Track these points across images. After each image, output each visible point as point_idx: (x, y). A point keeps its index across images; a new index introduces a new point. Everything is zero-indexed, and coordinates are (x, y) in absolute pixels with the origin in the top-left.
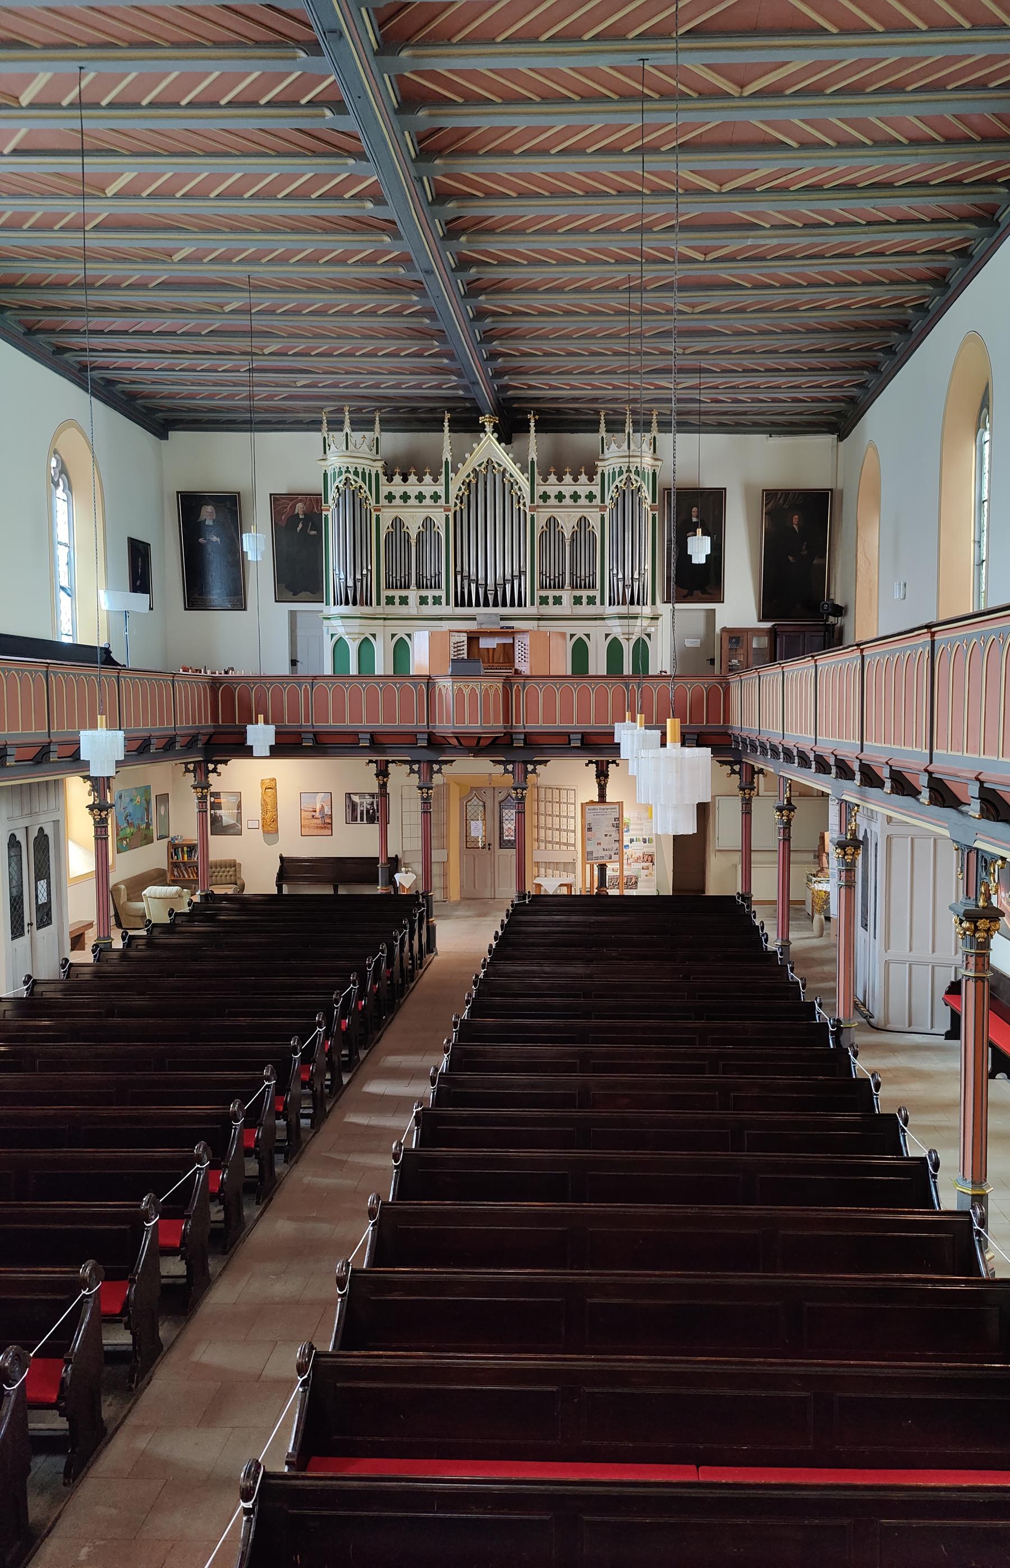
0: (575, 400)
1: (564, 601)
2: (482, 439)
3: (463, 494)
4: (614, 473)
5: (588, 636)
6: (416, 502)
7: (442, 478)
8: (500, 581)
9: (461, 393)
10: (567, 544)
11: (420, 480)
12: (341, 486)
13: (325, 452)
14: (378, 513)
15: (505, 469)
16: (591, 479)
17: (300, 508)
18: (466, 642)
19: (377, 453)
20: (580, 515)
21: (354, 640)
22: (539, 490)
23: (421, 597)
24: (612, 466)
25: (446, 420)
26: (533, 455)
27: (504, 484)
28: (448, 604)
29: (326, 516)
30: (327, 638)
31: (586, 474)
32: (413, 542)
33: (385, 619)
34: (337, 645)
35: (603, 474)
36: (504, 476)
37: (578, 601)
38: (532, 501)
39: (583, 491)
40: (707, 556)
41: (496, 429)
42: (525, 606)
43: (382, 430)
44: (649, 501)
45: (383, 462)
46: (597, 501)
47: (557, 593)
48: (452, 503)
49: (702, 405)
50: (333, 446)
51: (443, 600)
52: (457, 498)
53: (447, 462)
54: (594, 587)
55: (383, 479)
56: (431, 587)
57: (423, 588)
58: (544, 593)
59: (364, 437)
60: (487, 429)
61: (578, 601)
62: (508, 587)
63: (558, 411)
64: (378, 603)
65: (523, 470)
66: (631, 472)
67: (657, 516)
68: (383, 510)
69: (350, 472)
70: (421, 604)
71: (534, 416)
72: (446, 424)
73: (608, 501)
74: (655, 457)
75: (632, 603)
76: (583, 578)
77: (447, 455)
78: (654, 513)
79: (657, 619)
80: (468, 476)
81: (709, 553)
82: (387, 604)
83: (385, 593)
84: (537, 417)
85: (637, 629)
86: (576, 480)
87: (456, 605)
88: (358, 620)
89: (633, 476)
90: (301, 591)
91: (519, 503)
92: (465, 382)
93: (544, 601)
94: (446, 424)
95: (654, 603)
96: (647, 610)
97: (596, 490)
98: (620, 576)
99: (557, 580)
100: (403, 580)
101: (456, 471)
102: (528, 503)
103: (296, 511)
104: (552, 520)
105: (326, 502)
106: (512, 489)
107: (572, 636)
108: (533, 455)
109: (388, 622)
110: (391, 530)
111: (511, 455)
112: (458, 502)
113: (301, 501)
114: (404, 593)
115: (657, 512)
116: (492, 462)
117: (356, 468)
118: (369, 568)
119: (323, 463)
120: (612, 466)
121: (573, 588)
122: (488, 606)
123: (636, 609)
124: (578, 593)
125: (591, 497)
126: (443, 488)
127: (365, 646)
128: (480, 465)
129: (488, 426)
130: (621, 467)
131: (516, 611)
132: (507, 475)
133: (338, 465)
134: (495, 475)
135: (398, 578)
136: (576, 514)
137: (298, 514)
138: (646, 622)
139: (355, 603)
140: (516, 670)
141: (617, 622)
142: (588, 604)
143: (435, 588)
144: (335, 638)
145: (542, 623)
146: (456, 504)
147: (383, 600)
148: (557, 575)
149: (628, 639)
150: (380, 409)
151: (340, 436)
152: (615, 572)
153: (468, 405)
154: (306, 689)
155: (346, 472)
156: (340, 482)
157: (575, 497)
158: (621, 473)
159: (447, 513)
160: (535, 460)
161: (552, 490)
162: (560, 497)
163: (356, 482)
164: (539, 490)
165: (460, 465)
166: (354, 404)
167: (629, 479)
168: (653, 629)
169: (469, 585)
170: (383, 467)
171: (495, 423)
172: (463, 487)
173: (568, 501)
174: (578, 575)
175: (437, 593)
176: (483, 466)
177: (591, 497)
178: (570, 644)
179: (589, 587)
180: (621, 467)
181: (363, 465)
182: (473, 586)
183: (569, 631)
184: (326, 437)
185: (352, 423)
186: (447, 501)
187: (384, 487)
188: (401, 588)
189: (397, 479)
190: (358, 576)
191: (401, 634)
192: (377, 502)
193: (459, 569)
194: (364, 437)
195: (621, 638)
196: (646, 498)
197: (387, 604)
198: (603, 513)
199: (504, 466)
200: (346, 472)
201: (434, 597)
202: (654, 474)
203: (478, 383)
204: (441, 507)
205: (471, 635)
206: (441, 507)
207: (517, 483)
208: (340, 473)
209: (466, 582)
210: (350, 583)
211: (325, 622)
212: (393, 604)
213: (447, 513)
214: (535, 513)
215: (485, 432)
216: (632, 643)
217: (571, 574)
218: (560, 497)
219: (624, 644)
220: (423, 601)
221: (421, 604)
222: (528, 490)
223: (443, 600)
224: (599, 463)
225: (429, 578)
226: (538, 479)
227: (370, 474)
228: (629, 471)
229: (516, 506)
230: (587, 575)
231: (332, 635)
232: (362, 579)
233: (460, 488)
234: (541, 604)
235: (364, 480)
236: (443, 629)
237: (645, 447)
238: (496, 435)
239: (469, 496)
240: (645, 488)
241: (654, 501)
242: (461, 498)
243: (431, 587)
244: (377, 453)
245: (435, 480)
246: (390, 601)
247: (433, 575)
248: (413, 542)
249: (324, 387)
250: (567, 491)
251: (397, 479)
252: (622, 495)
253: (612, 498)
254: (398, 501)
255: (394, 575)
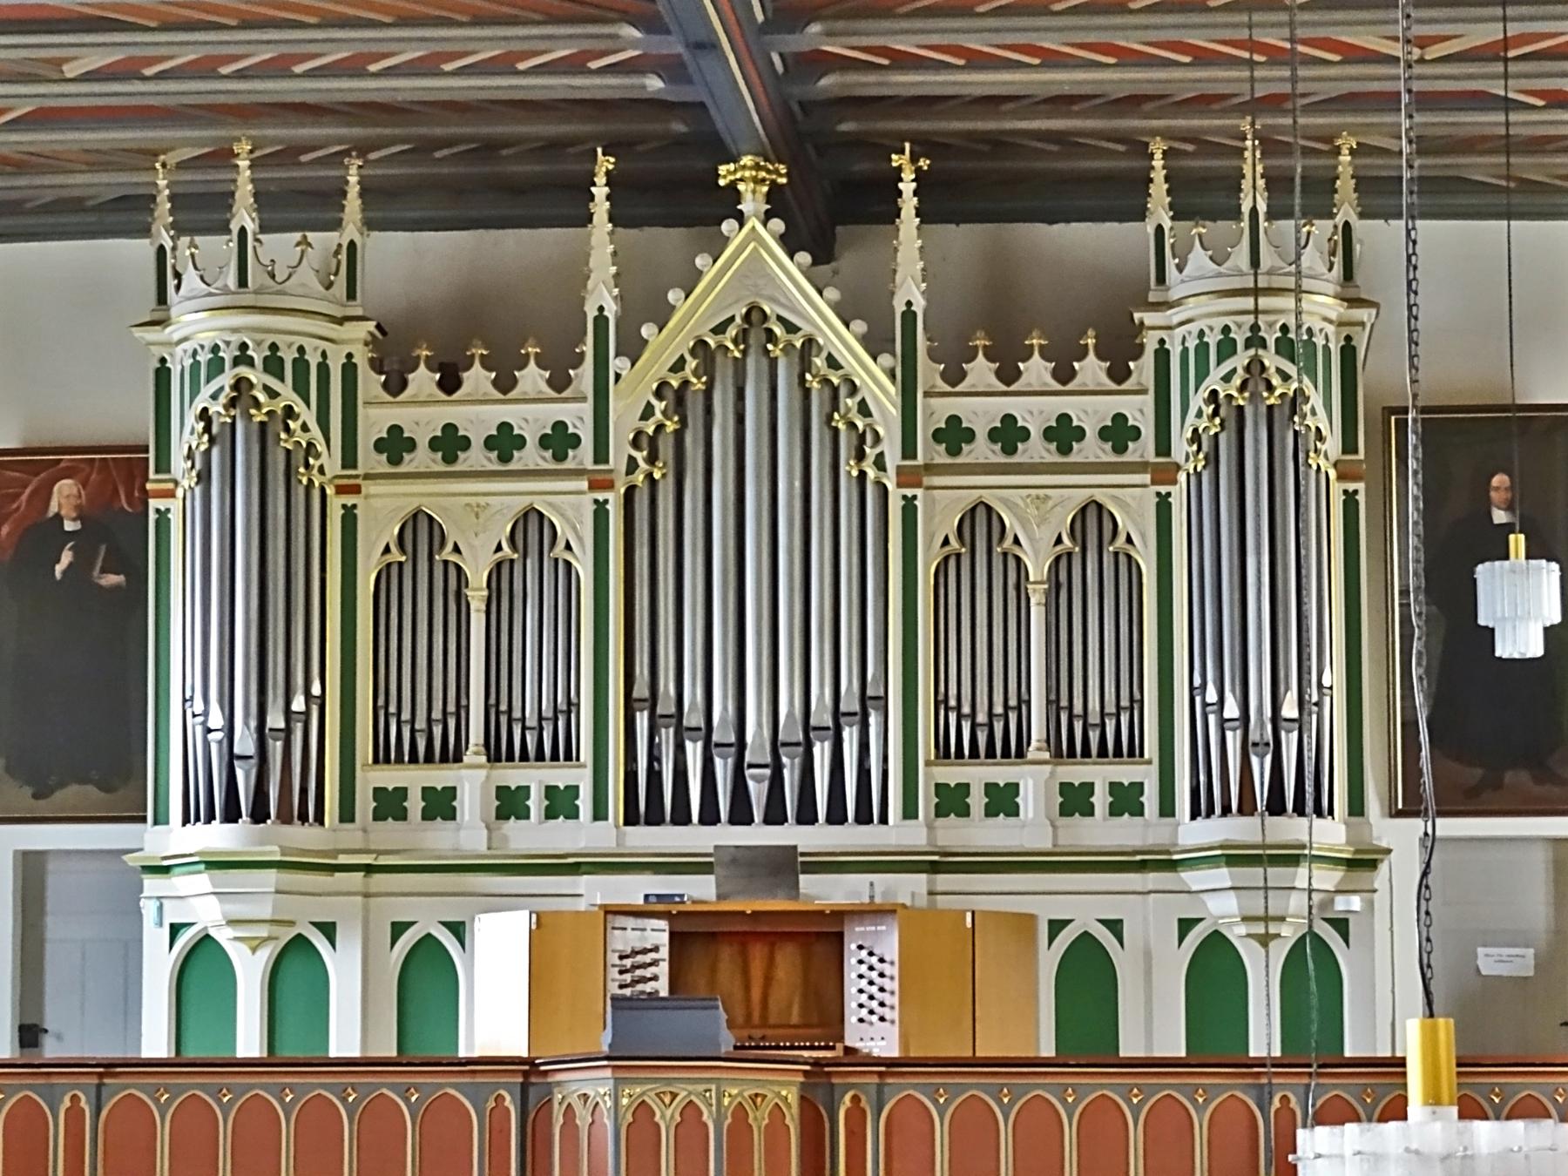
0: (1062, 102)
1: (1028, 800)
2: (726, 240)
3: (660, 427)
4: (1203, 348)
5: (1115, 926)
6: (489, 461)
7: (584, 375)
8: (791, 731)
9: (654, 84)
10: (1037, 598)
11: (505, 384)
12: (216, 408)
13: (162, 299)
14: (349, 500)
15: (810, 342)
16: (1119, 373)
17: (64, 496)
18: (664, 953)
19: (351, 294)
20: (1082, 496)
21: (255, 945)
22: (934, 412)
23: (502, 792)
24: (1194, 328)
25: (601, 179)
26: (910, 292)
27: (807, 393)
28: (599, 814)
29: (163, 515)
30: (154, 939)
31: (1100, 356)
32: (477, 598)
33: (369, 869)
34: (186, 979)
35: (1162, 355)
36: (805, 365)
37: (1075, 801)
38: (909, 450)
39: (1090, 412)
40: (1548, 631)
41: (777, 204)
42: (884, 820)
43: (370, 224)
44: (1333, 444)
45: (371, 326)
46: (1145, 448)
47: (1001, 773)
48: (617, 459)
49: (1513, 117)
50: (191, 279)
51: (585, 803)
52: (635, 443)
53: (601, 321)
54: (1134, 751)
55: (370, 383)
56: (540, 756)
57: (510, 758)
58: (952, 774)
59: (304, 242)
60: (745, 207)
61: (1075, 801)
62: (822, 753)
63: (999, 144)
64: (347, 815)
65: (875, 344)
66: (1264, 345)
67: (1361, 498)
68: (369, 487)
69: (250, 362)
70: (502, 815)
71: (914, 159)
72: (600, 191)
73: (1180, 447)
74: (1351, 293)
75: (1276, 806)
76: (1094, 718)
77: (602, 297)
78: (1351, 487)
79: (1373, 865)
80: (679, 365)
81: (1556, 618)
82: (379, 816)
83: (371, 778)
84: (924, 163)
85: (1296, 903)
86: (1064, 374)
87: (631, 819)
88: (272, 874)
89: (1271, 360)
90: (62, 785)
91: (861, 456)
92: (673, 46)
93: (952, 801)
94: (600, 191)
95: (1357, 807)
96: (1331, 834)
97: (1139, 409)
98: (1232, 710)
99: (998, 727)
100: (437, 731)
101: (633, 348)
102: (893, 459)
103: (53, 508)
104: (981, 515)
105: (163, 465)
106: (835, 408)
107: (1056, 926)
108: (910, 292)
109: (379, 879)
110: (396, 556)
111: (832, 293)
112: (640, 456)
113: (68, 473)
114: (439, 776)
115: (1361, 486)
116: (765, 317)
117: (274, 347)
118: (316, 690)
119: (152, 334)
120: (1194, 328)
121: (1058, 754)
122: (749, 821)
123: (1290, 829)
124: (1077, 773)
125: (1119, 433)
126: (587, 409)
127: (293, 966)
128: (719, 330)
129: (748, 196)
130: (1226, 330)
131: (850, 837)
132: (819, 362)
133: (207, 338)
134: (773, 363)
135: (421, 724)
136: (1069, 495)
137: (58, 518)
138: (1327, 878)
139: (260, 815)
140: (849, 1051)
141: (1222, 876)
142: (1115, 811)
143: (555, 757)
144: (185, 939)
145: (944, 881)
146: (632, 461)
147: (365, 804)
148: (999, 709)
149: (1265, 940)
150: (363, 149)
151: (219, 247)
152: (1212, 696)
153: (679, 127)
154: (75, 1114)
155: (236, 362)
156: (212, 396)
157: (1064, 433)
158: (1227, 348)
159: (601, 496)
160: (919, 306)
161: (982, 413)
162: (1009, 434)
163: (273, 394)
164: (934, 412)
165: (647, 331)
166: (270, 132)
167: (1256, 368)
168: (1356, 902)
169: (680, 749)
170: (371, 342)
171: (773, 182)
172: (659, 406)
173: (1036, 449)
174: (1078, 708)
175: (561, 776)
176: (732, 331)
177: (1119, 433)
178: (1049, 959)
179: (1118, 752)
180: (1226, 330)
181: (294, 335)
182: (694, 751)
183: (1047, 910)
184: (168, 244)
185: (262, 199)
186: (601, 454)
187: (374, 412)
188: (429, 759)
189: (423, 380)
190: (275, 720)
191: (428, 921)
192: (349, 460)
193: (641, 690)
194: (304, 242)
195: (1236, 933)
196: (1319, 436)
197: (379, 816)
198: (1163, 489)
199: (807, 329)
200: (236, 362)
201: (550, 791)
202: (1348, 351)
203: (715, 46)
204: (578, 473)
205: (683, 927)
206: (578, 473)
207: (854, 390)
208: (216, 367)
209: (667, 736)
210: (245, 743)
211: (151, 884)
212: (402, 815)
213: (601, 496)
214: (919, 492)
215: (741, 218)
216: (1280, 952)
217: (1053, 704)
218: (1009, 434)
219: (1250, 955)
220: (510, 804)
221: (502, 815)
222: (895, 412)
223: (585, 803)
224: (1149, 318)
225: (532, 721)
226: (928, 372)
227: (323, 369)
228: (1255, 341)
229: (848, 468)
230: (1110, 708)
231: (175, 930)
232: (288, 731)
233: (649, 407)
234: (940, 812)
235: (301, 389)
236: (581, 905)
237: (1312, 259)
238: (778, 225)
239: (679, 436)
240: (1316, 399)
241: (1349, 446)
242: (653, 441)
243: (540, 756)
244: (351, 294)
245: (560, 383)
246: (390, 805)
247: (547, 711)
248: (477, 598)
249: (161, 76)
250: (1033, 413)
251: (423, 380)
252: (1232, 425)
253: (1196, 437)
254: (422, 459)
255: (406, 715)
